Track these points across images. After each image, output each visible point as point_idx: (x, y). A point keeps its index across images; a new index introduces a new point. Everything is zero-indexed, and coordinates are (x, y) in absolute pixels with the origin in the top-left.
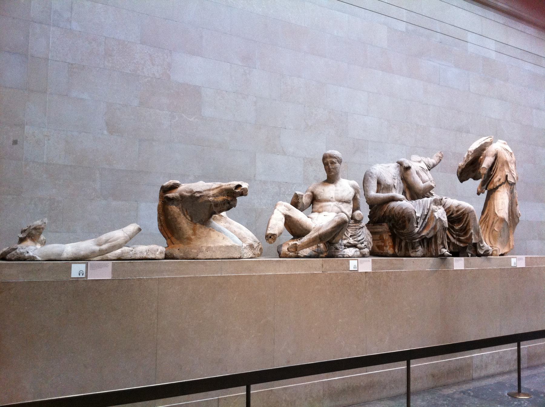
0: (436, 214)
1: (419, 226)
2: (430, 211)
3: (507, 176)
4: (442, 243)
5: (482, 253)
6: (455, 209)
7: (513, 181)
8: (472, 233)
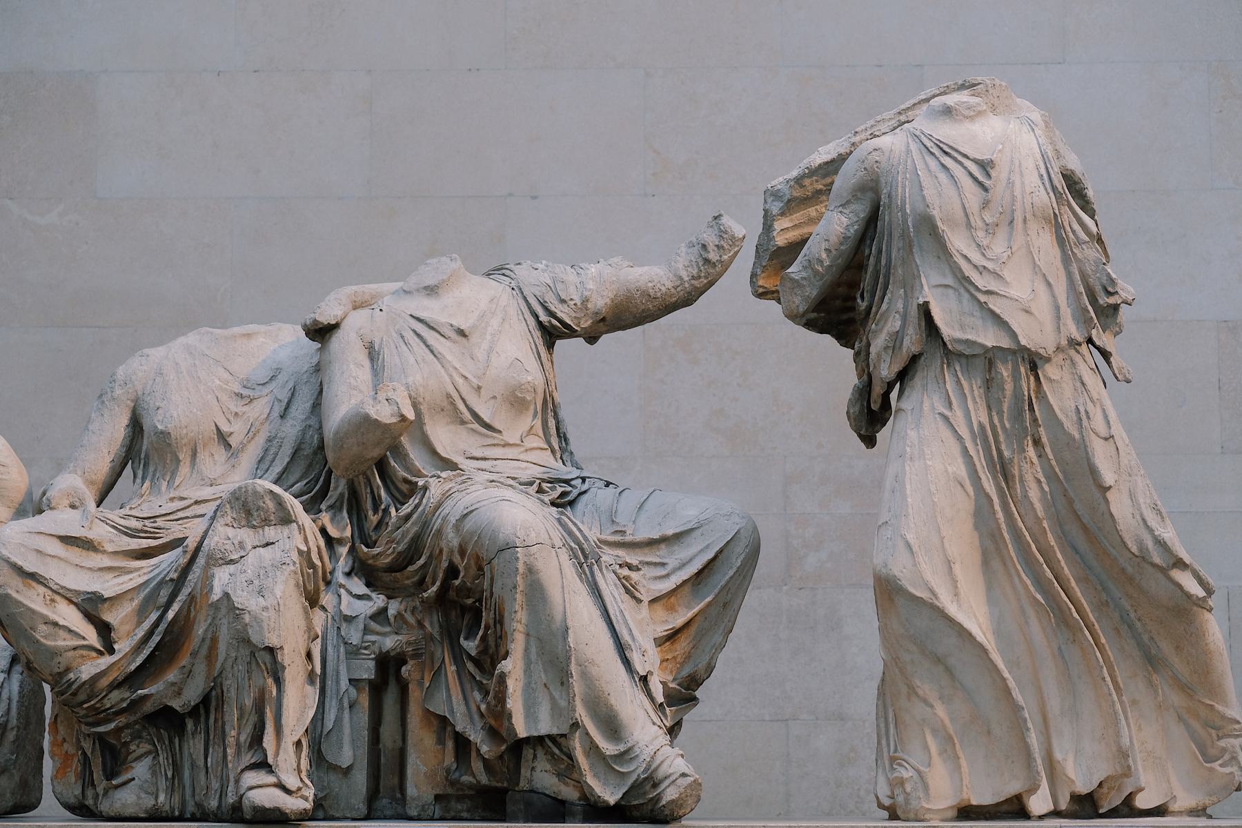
0: (222, 579)
1: (123, 646)
2: (201, 561)
3: (925, 312)
4: (257, 739)
5: (610, 795)
6: (455, 543)
7: (989, 338)
8: (502, 678)
